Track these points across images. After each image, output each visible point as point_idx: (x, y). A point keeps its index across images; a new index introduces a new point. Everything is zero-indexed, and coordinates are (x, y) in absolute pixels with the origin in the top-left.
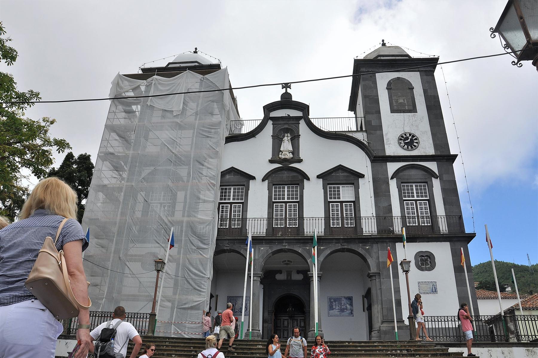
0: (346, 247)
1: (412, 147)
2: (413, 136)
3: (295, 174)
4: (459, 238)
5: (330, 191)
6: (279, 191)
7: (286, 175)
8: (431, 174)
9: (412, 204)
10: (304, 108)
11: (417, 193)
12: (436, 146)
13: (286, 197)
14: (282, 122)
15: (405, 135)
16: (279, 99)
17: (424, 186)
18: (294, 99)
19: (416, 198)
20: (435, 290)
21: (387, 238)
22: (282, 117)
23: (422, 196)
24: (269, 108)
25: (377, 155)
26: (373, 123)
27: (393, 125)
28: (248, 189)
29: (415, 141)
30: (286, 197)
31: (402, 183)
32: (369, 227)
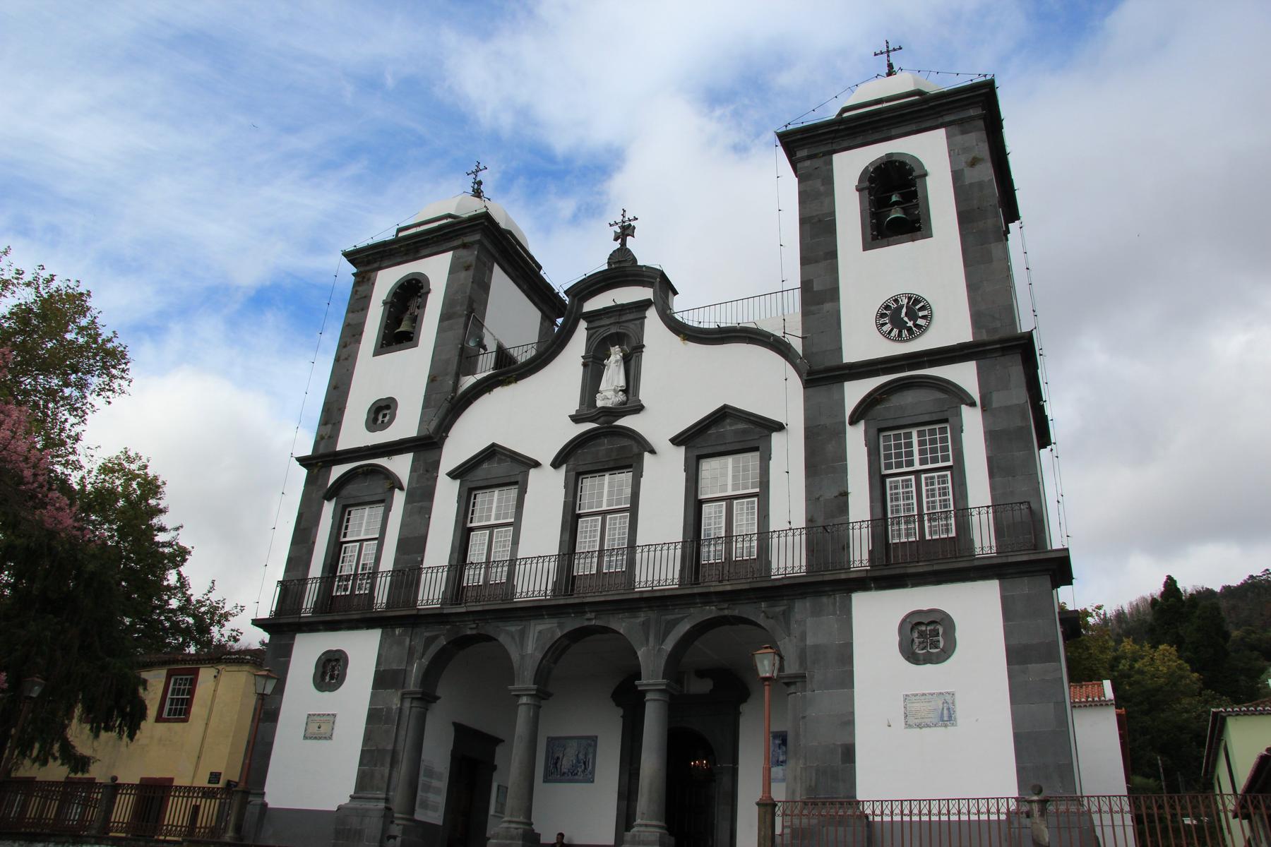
0: (726, 612)
1: (910, 329)
2: (917, 301)
3: (626, 442)
4: (1031, 564)
8: (958, 395)
11: (922, 452)
12: (977, 319)
14: (607, 322)
15: (896, 301)
17: (943, 430)
19: (917, 466)
20: (950, 717)
21: (830, 583)
22: (605, 309)
23: (934, 460)
25: (816, 368)
26: (817, 287)
29: (921, 314)
31: (880, 430)
32: (789, 559)
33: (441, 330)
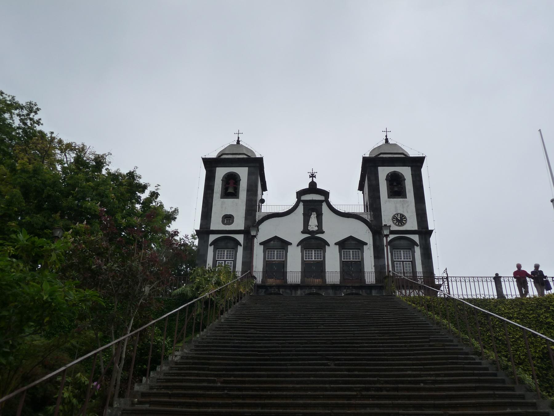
2: (403, 216)
5: (344, 254)
6: (309, 253)
7: (313, 241)
8: (414, 243)
9: (400, 264)
10: (326, 194)
11: (404, 256)
13: (313, 257)
16: (308, 187)
18: (318, 187)
19: (403, 260)
23: (407, 259)
24: (300, 194)
27: (389, 207)
28: (287, 252)
30: (313, 257)
33: (248, 195)
